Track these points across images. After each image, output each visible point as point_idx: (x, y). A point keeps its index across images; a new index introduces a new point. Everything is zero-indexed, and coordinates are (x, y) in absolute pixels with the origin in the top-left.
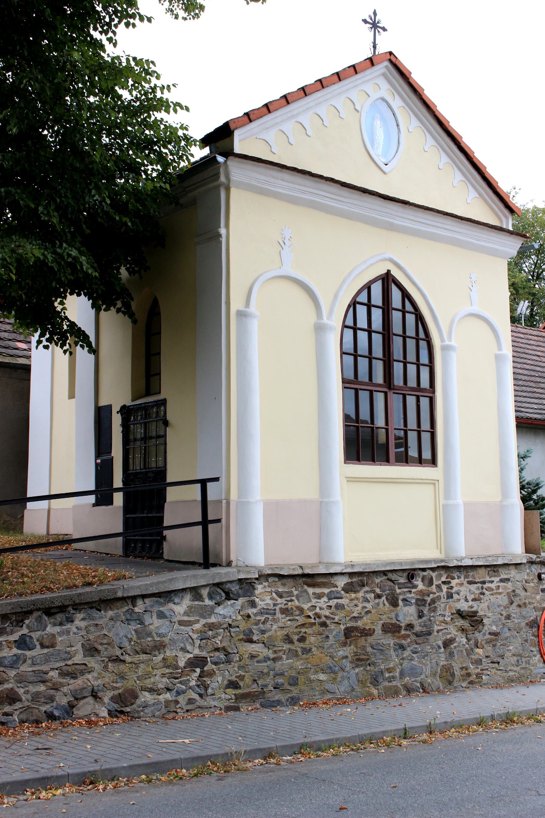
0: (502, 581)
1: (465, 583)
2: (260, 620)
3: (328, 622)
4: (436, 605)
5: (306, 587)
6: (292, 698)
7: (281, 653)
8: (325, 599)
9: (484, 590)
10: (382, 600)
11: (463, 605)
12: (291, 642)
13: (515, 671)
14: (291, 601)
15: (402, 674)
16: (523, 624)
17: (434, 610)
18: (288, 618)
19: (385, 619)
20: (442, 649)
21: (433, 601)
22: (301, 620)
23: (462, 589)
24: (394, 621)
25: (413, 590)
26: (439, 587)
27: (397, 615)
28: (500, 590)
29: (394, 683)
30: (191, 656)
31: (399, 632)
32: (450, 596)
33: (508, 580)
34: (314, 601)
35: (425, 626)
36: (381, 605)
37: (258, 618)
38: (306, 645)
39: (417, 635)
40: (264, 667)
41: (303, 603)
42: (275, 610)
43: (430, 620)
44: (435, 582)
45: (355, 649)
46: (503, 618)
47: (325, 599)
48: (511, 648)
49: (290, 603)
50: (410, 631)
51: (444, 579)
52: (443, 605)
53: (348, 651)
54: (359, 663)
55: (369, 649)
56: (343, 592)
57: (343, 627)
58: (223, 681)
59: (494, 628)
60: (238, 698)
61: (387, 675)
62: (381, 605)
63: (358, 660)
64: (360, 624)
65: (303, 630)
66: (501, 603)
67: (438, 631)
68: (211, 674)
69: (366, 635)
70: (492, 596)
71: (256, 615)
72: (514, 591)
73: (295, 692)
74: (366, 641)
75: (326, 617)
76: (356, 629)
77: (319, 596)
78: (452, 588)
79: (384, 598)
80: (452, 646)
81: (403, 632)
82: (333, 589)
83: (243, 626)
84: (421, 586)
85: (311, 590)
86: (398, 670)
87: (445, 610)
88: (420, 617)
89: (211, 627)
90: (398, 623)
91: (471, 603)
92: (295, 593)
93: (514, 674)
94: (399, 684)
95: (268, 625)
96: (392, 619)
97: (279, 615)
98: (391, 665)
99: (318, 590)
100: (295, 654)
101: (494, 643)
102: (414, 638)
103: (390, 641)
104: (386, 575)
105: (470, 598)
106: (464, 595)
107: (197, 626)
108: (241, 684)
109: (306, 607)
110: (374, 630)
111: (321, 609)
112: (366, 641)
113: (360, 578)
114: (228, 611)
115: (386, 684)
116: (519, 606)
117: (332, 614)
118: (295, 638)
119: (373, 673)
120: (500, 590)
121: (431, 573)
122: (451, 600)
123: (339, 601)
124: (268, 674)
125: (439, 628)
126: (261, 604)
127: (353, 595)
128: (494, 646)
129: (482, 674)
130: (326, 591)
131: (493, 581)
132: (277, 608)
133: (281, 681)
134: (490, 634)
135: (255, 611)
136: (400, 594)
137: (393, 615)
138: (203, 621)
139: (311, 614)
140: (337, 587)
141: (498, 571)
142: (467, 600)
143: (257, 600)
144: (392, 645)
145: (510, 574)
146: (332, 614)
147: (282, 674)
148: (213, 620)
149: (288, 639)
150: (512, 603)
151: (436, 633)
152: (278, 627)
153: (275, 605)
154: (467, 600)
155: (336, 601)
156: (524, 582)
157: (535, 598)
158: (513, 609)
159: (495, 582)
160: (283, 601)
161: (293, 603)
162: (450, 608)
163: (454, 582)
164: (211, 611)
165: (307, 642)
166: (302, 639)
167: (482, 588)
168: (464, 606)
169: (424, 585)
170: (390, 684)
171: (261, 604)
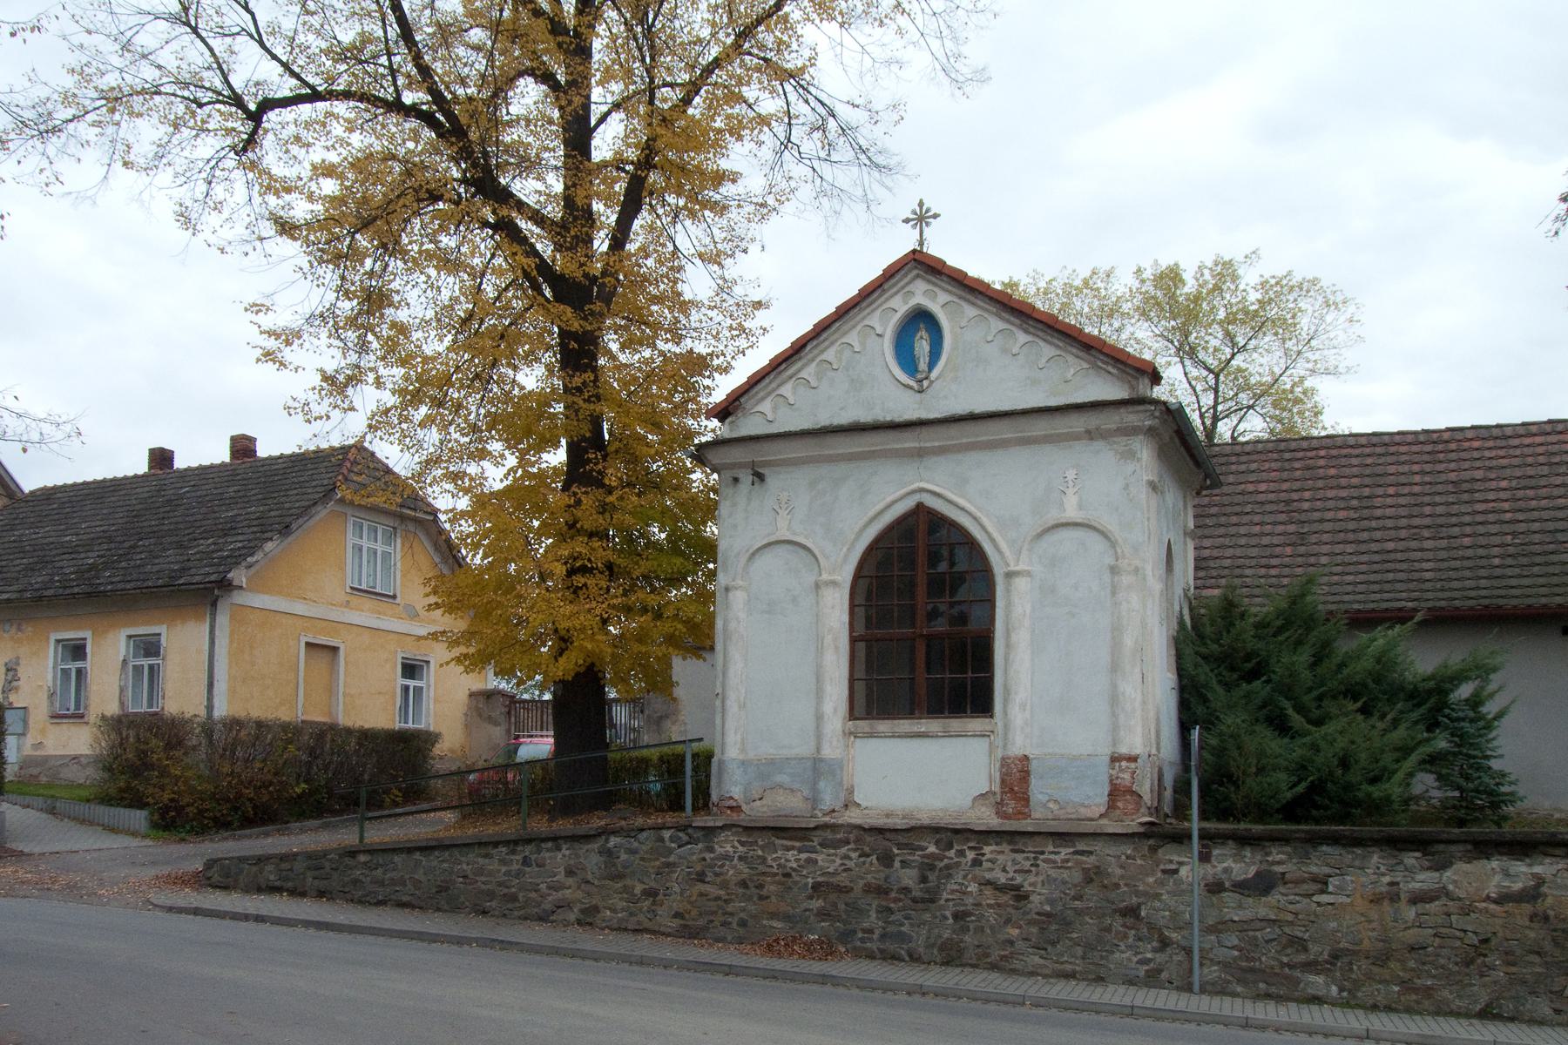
12: (747, 887)
15: (883, 936)
17: (950, 876)
20: (951, 921)
21: (947, 867)
22: (762, 868)
23: (1001, 858)
26: (961, 853)
31: (887, 893)
32: (977, 863)
33: (1091, 853)
38: (764, 892)
39: (915, 901)
53: (817, 904)
55: (842, 907)
77: (788, 849)
81: (893, 895)
83: (698, 868)
85: (778, 842)
89: (668, 865)
91: (1011, 874)
100: (749, 899)
123: (813, 856)
130: (797, 844)
142: (1004, 870)
148: (671, 859)
150: (1091, 881)
152: (735, 871)
154: (1004, 870)
158: (1089, 891)
163: (987, 849)
166: (760, 887)
168: (1002, 879)
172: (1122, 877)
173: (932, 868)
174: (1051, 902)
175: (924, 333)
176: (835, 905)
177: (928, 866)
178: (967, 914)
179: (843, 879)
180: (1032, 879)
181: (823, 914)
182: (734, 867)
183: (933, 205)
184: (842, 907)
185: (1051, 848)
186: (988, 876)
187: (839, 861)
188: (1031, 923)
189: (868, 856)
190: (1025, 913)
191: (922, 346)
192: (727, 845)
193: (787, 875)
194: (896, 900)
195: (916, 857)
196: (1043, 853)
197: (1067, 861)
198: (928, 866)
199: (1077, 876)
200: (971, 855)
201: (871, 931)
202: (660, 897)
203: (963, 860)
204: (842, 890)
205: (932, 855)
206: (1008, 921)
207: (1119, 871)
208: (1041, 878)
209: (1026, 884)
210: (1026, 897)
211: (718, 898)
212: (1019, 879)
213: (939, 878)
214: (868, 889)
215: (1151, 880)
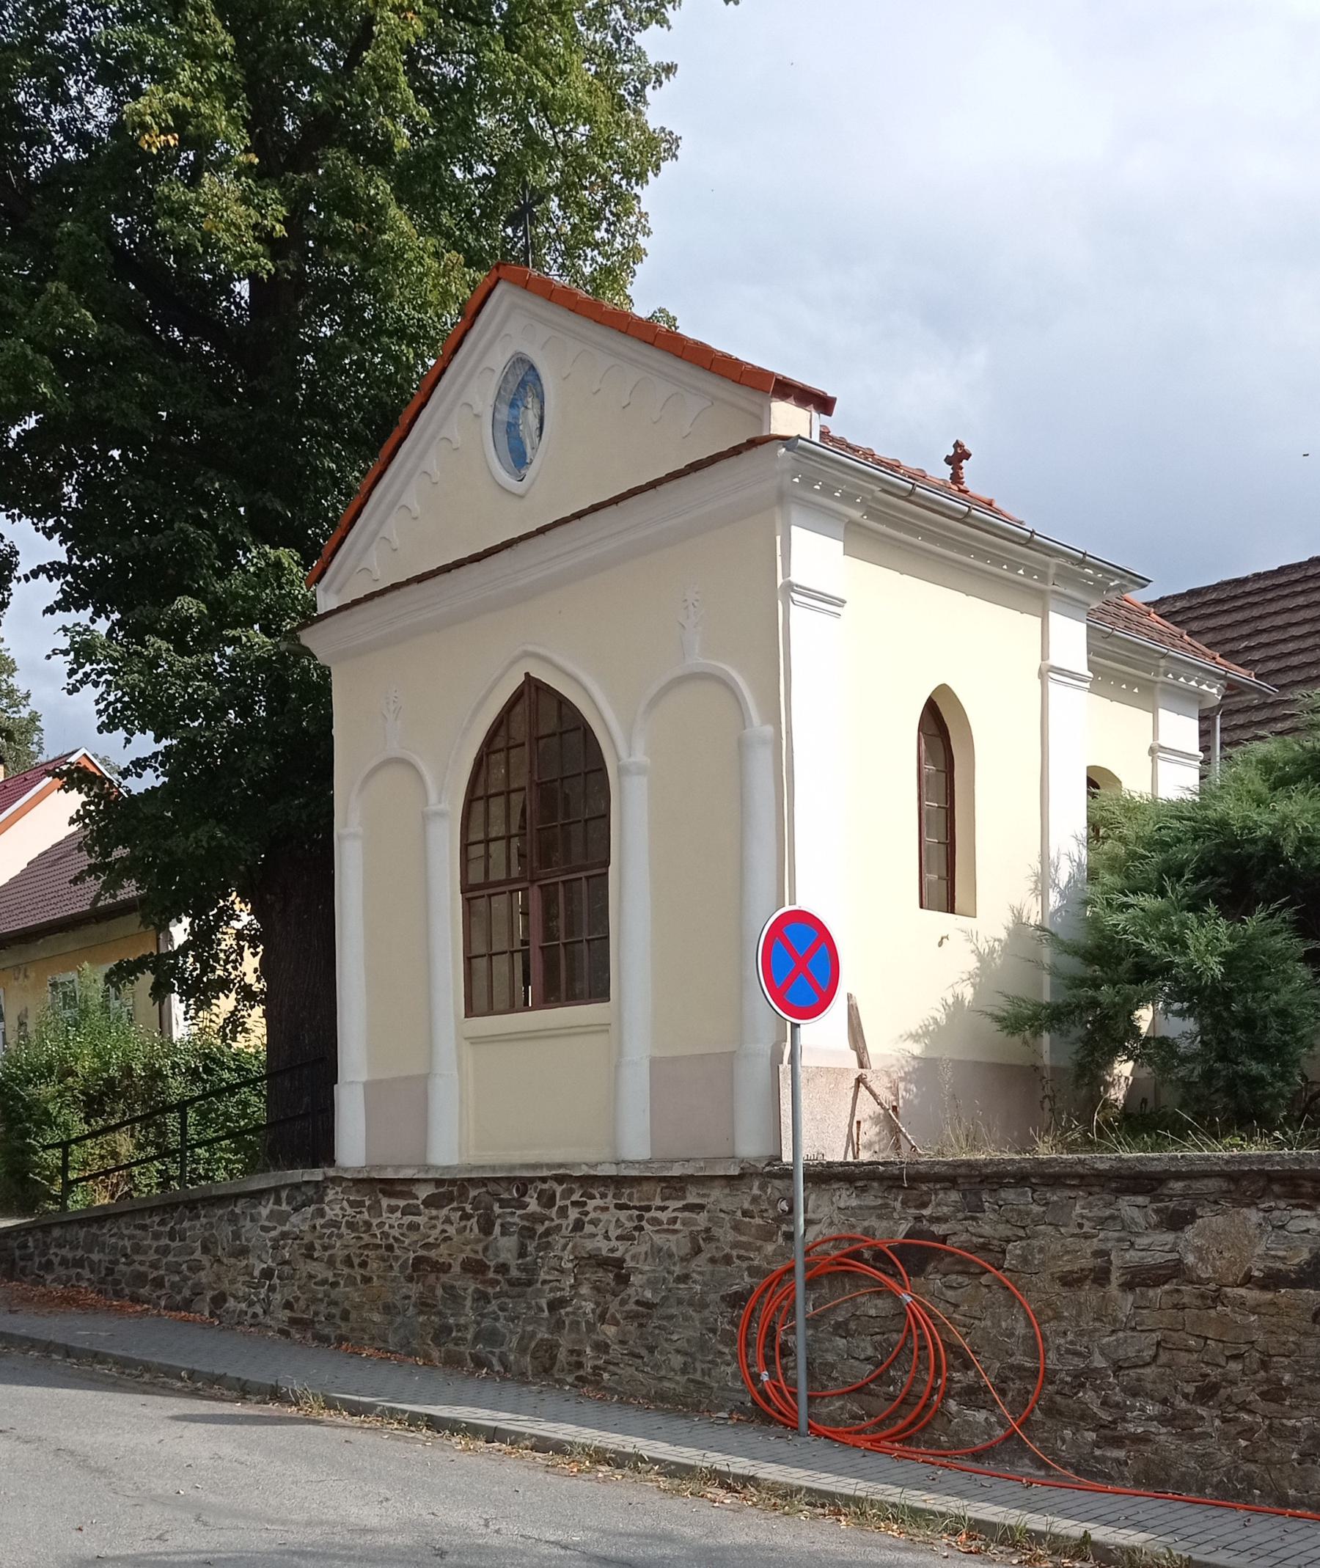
0: (687, 1208)
1: (612, 1206)
3: (396, 1245)
4: (550, 1239)
5: (380, 1196)
8: (398, 1214)
9: (644, 1223)
10: (469, 1223)
11: (599, 1245)
12: (351, 1266)
14: (360, 1212)
15: (477, 1338)
16: (713, 1297)
17: (548, 1246)
20: (546, 1314)
21: (547, 1233)
24: (480, 1256)
25: (519, 1212)
26: (563, 1212)
28: (678, 1226)
31: (483, 1273)
32: (578, 1226)
35: (524, 1270)
39: (511, 1283)
44: (559, 1203)
47: (398, 1214)
51: (575, 1197)
52: (563, 1241)
53: (414, 1290)
54: (424, 1309)
55: (439, 1292)
57: (412, 1255)
59: (648, 1294)
60: (293, 1321)
63: (423, 1304)
64: (432, 1254)
67: (544, 1282)
70: (658, 1236)
71: (322, 1227)
72: (708, 1230)
73: (345, 1329)
74: (438, 1278)
75: (394, 1238)
77: (392, 1210)
78: (587, 1214)
80: (563, 1312)
81: (491, 1275)
84: (533, 1206)
85: (385, 1202)
86: (471, 1330)
91: (614, 1243)
93: (673, 1386)
96: (476, 1252)
97: (343, 1229)
98: (462, 1321)
99: (394, 1202)
101: (644, 1321)
102: (506, 1287)
103: (470, 1286)
104: (485, 1185)
105: (614, 1233)
106: (605, 1227)
107: (273, 1234)
111: (391, 1227)
112: (438, 1278)
115: (451, 1346)
116: (713, 1260)
118: (356, 1261)
120: (678, 1226)
121: (555, 1185)
122: (579, 1234)
123: (415, 1219)
125: (548, 1278)
126: (330, 1214)
127: (434, 1212)
130: (402, 1203)
135: (322, 1221)
136: (499, 1216)
137: (480, 1247)
138: (280, 1229)
141: (683, 1190)
142: (607, 1238)
143: (327, 1208)
144: (470, 1291)
146: (402, 1235)
149: (348, 1262)
150: (697, 1251)
151: (539, 1285)
154: (607, 1238)
155: (411, 1218)
156: (739, 1213)
157: (759, 1249)
163: (592, 1204)
167: (640, 1218)
168: (603, 1246)
170: (456, 1348)
171: (330, 1214)
172: (735, 1245)
174: (652, 1283)
180: (634, 1250)
182: (340, 1236)
185: (658, 1202)
190: (623, 1302)
192: (336, 1206)
193: (390, 1248)
196: (648, 1209)
200: (573, 1214)
203: (564, 1223)
207: (731, 1236)
208: (645, 1248)
209: (628, 1258)
213: (538, 1249)
215: (770, 1248)
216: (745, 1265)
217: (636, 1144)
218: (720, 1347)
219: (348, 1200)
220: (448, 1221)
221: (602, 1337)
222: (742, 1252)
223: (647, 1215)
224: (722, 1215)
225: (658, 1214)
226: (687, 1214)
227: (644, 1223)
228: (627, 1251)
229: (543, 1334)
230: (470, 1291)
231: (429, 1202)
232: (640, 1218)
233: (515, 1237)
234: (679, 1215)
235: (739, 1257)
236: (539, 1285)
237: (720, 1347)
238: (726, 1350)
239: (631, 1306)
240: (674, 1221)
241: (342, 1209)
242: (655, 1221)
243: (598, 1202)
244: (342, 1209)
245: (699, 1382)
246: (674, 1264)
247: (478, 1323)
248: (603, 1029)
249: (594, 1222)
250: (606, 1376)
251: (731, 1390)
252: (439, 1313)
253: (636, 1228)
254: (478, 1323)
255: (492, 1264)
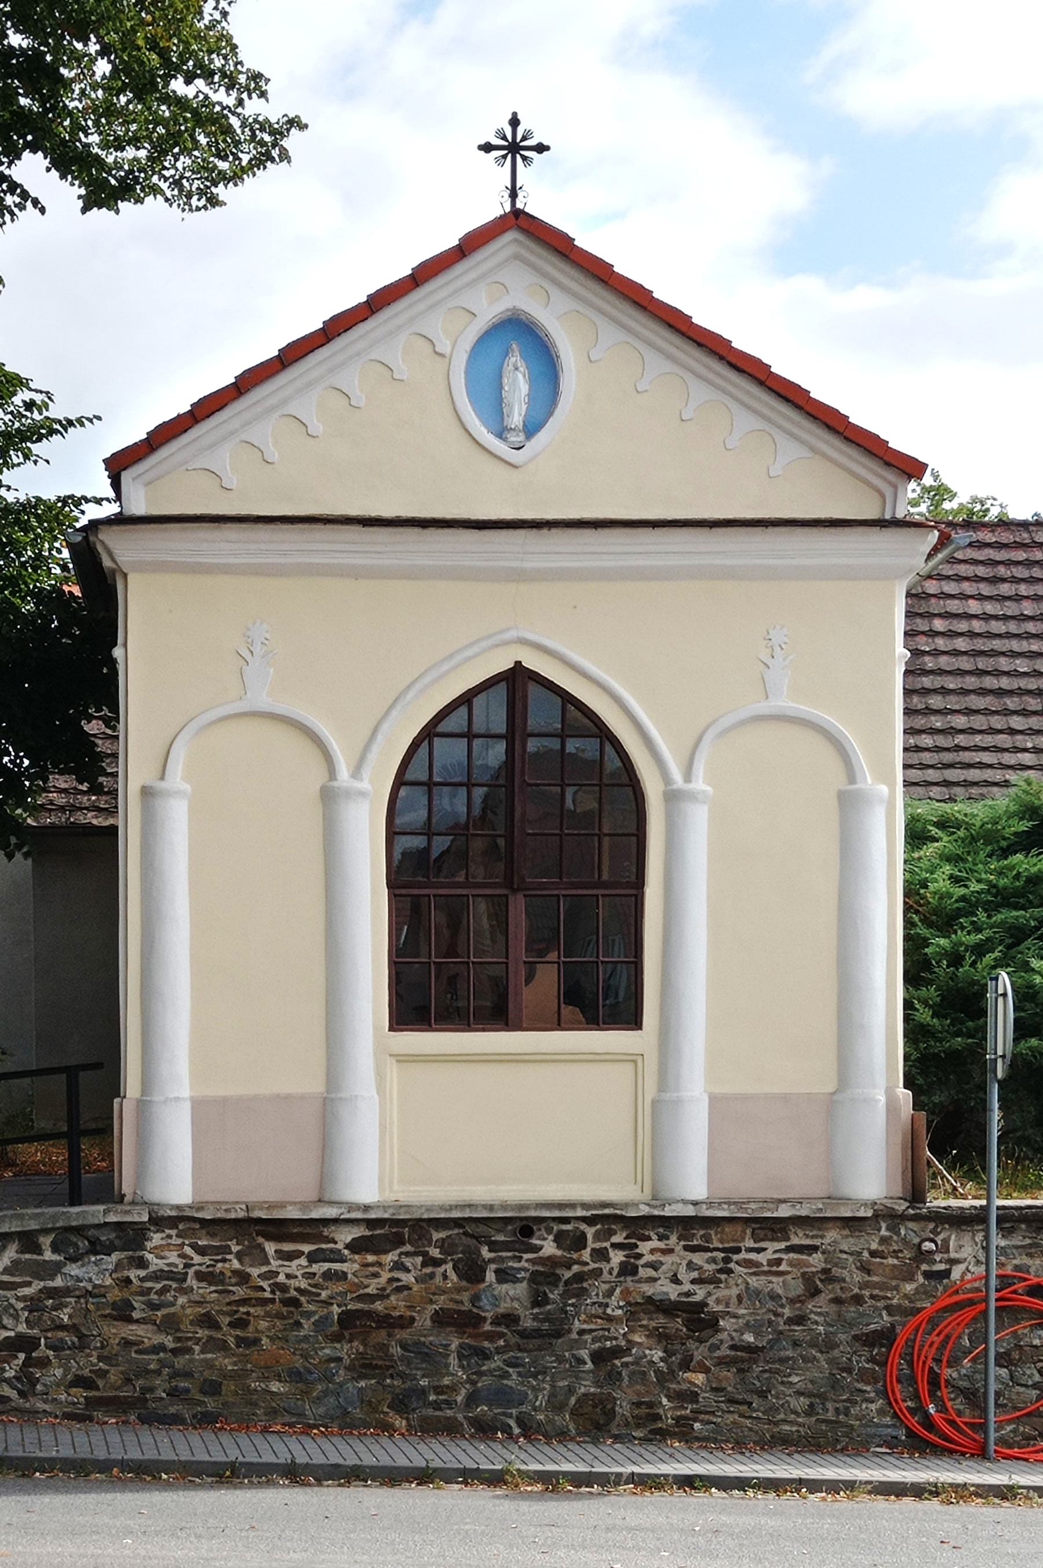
1: (678, 1249)
2: (152, 1288)
4: (585, 1285)
5: (260, 1240)
6: (205, 1414)
7: (190, 1343)
8: (303, 1261)
9: (732, 1265)
10: (441, 1269)
11: (664, 1289)
13: (799, 1425)
14: (224, 1260)
15: (472, 1400)
17: (582, 1293)
18: (213, 1288)
19: (442, 1302)
20: (589, 1365)
21: (579, 1277)
22: (240, 1292)
23: (668, 1259)
24: (467, 1306)
25: (526, 1256)
26: (601, 1255)
27: (475, 1299)
28: (783, 1267)
29: (449, 1413)
30: (12, 1334)
32: (628, 1269)
33: (814, 1249)
34: (275, 1264)
36: (438, 1279)
37: (149, 1284)
38: (249, 1333)
39: (524, 1334)
40: (152, 1362)
41: (251, 1266)
42: (187, 1273)
43: (566, 1312)
44: (591, 1244)
45: (361, 1349)
46: (781, 1321)
47: (303, 1261)
48: (795, 1379)
49: (220, 1265)
50: (507, 1327)
51: (617, 1239)
52: (605, 1287)
53: (345, 1350)
55: (396, 1351)
56: (346, 1252)
58: (65, 1375)
59: (749, 1338)
61: (432, 1398)
62: (438, 1279)
63: (364, 1366)
64: (379, 1306)
65: (242, 1309)
66: (780, 1291)
67: (581, 1333)
68: (44, 1363)
69: (392, 1326)
70: (754, 1279)
71: (142, 1280)
72: (825, 1271)
73: (211, 1404)
76: (369, 1314)
77: (290, 1256)
78: (640, 1256)
79: (449, 1267)
80: (617, 1362)
81: (487, 1327)
82: (324, 1246)
83: (115, 1295)
84: (549, 1248)
85: (270, 1248)
86: (463, 1391)
87: (610, 1293)
88: (536, 1304)
90: (475, 1310)
91: (687, 1287)
92: (235, 1248)
93: (794, 1429)
94: (460, 1417)
95: (169, 1296)
97: (191, 1281)
98: (446, 1381)
100: (222, 1346)
101: (745, 1366)
102: (514, 1340)
104: (462, 1227)
105: (683, 1275)
106: (671, 1272)
108: (101, 1383)
109: (255, 1272)
110: (413, 1319)
111: (288, 1276)
112: (389, 1335)
113: (390, 1232)
114: (93, 1272)
115: (430, 1412)
116: (837, 1301)
117: (315, 1286)
119: (397, 1391)
120: (783, 1267)
121: (583, 1227)
122: (629, 1279)
124: (158, 1373)
125: (585, 1326)
127: (371, 1258)
128: (740, 1371)
129: (695, 1420)
130: (307, 1248)
131: (765, 1249)
132: (191, 1272)
133: (183, 1384)
134: (733, 1347)
135: (142, 1273)
136: (491, 1261)
137: (465, 1297)
138: (37, 1285)
139: (265, 1284)
140: (336, 1243)
142: (675, 1280)
143: (150, 1257)
144: (453, 1347)
145: (822, 1237)
146: (315, 1286)
147: (188, 1375)
148: (58, 1282)
149: (208, 1321)
150: (815, 1292)
151: (574, 1336)
153: (187, 1266)
154: (675, 1280)
155: (326, 1266)
156: (866, 1254)
157: (896, 1288)
158: (819, 1307)
159: (770, 1251)
160: (206, 1260)
161: (227, 1265)
162: (626, 1293)
163: (644, 1247)
164: (55, 1269)
165: (251, 1328)
166: (240, 1323)
168: (673, 1292)
169: (558, 1247)
170: (438, 1413)
171: (156, 1263)
172: (863, 1286)
173: (553, 1280)
174: (755, 1328)
175: (515, 358)
176: (384, 1348)
177: (545, 1276)
178: (617, 1352)
179: (397, 1304)
180: (722, 1293)
181: (363, 1367)
183: (537, 126)
184: (396, 1351)
185: (750, 1244)
186: (648, 1289)
187: (385, 1276)
188: (721, 1362)
189: (436, 1263)
190: (715, 1347)
191: (518, 386)
192: (163, 1252)
193: (295, 1303)
194: (491, 1337)
195: (525, 1263)
196: (738, 1250)
197: (778, 1262)
198: (545, 1276)
199: (797, 1288)
200: (617, 1257)
201: (453, 1388)
202: (43, 1351)
203: (605, 1267)
204: (389, 1322)
205: (551, 1260)
206: (686, 1365)
207: (858, 1277)
208: (734, 1291)
209: (711, 1301)
210: (712, 1324)
211: (161, 1348)
212: (700, 1293)
213: (566, 1295)
214: (441, 1319)
215: (909, 1288)
216: (881, 1304)
217: (693, 1184)
218: (860, 1386)
219: (193, 1246)
220: (399, 1266)
221: (684, 1386)
222: (876, 1292)
223: (735, 1257)
224: (845, 1256)
225: (753, 1256)
226: (792, 1255)
227: (732, 1265)
228: (709, 1294)
229: (587, 1387)
230: (453, 1347)
231: (355, 1246)
232: (727, 1260)
233: (525, 1284)
234: (783, 1256)
235: (872, 1297)
236: (574, 1336)
237: (860, 1386)
238: (868, 1388)
239: (724, 1351)
240: (778, 1262)
241: (183, 1256)
242: (748, 1263)
243: (655, 1243)
244: (183, 1256)
245: (832, 1422)
246: (782, 1306)
247: (474, 1383)
248: (634, 1060)
249: (654, 1266)
250: (697, 1426)
251: (877, 1425)
252: (402, 1376)
253: (720, 1271)
254: (474, 1383)
255: (488, 1315)
